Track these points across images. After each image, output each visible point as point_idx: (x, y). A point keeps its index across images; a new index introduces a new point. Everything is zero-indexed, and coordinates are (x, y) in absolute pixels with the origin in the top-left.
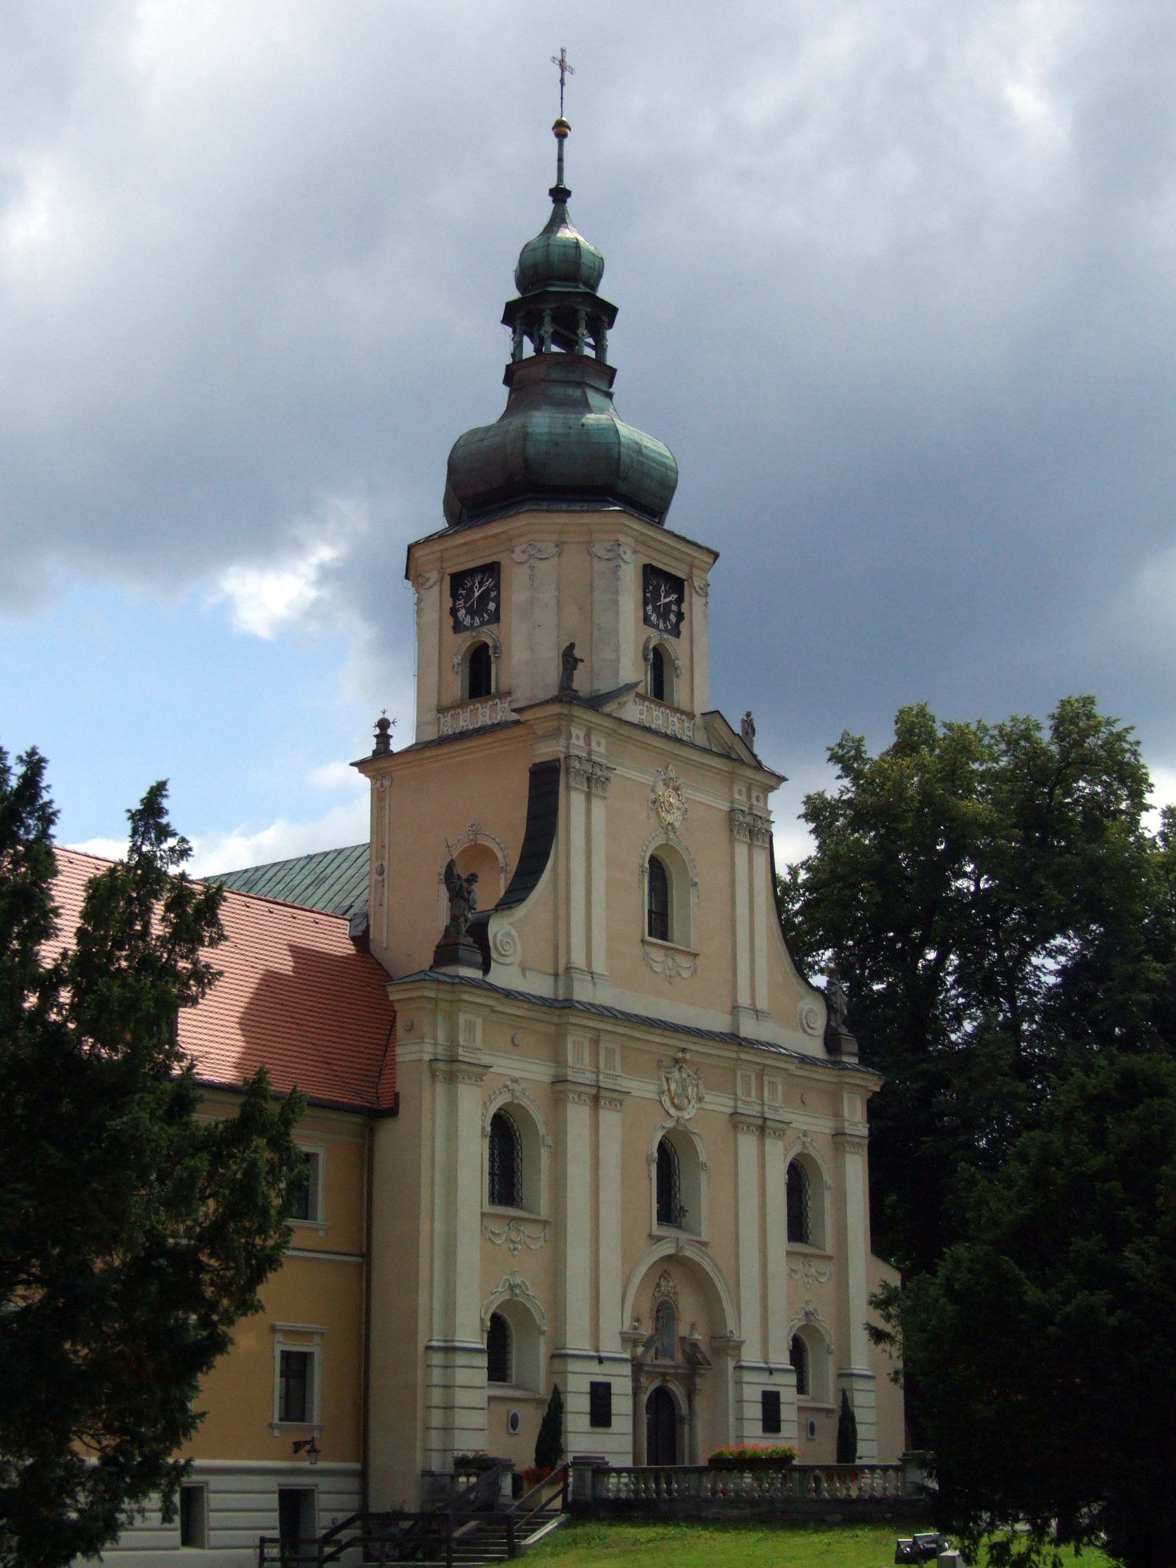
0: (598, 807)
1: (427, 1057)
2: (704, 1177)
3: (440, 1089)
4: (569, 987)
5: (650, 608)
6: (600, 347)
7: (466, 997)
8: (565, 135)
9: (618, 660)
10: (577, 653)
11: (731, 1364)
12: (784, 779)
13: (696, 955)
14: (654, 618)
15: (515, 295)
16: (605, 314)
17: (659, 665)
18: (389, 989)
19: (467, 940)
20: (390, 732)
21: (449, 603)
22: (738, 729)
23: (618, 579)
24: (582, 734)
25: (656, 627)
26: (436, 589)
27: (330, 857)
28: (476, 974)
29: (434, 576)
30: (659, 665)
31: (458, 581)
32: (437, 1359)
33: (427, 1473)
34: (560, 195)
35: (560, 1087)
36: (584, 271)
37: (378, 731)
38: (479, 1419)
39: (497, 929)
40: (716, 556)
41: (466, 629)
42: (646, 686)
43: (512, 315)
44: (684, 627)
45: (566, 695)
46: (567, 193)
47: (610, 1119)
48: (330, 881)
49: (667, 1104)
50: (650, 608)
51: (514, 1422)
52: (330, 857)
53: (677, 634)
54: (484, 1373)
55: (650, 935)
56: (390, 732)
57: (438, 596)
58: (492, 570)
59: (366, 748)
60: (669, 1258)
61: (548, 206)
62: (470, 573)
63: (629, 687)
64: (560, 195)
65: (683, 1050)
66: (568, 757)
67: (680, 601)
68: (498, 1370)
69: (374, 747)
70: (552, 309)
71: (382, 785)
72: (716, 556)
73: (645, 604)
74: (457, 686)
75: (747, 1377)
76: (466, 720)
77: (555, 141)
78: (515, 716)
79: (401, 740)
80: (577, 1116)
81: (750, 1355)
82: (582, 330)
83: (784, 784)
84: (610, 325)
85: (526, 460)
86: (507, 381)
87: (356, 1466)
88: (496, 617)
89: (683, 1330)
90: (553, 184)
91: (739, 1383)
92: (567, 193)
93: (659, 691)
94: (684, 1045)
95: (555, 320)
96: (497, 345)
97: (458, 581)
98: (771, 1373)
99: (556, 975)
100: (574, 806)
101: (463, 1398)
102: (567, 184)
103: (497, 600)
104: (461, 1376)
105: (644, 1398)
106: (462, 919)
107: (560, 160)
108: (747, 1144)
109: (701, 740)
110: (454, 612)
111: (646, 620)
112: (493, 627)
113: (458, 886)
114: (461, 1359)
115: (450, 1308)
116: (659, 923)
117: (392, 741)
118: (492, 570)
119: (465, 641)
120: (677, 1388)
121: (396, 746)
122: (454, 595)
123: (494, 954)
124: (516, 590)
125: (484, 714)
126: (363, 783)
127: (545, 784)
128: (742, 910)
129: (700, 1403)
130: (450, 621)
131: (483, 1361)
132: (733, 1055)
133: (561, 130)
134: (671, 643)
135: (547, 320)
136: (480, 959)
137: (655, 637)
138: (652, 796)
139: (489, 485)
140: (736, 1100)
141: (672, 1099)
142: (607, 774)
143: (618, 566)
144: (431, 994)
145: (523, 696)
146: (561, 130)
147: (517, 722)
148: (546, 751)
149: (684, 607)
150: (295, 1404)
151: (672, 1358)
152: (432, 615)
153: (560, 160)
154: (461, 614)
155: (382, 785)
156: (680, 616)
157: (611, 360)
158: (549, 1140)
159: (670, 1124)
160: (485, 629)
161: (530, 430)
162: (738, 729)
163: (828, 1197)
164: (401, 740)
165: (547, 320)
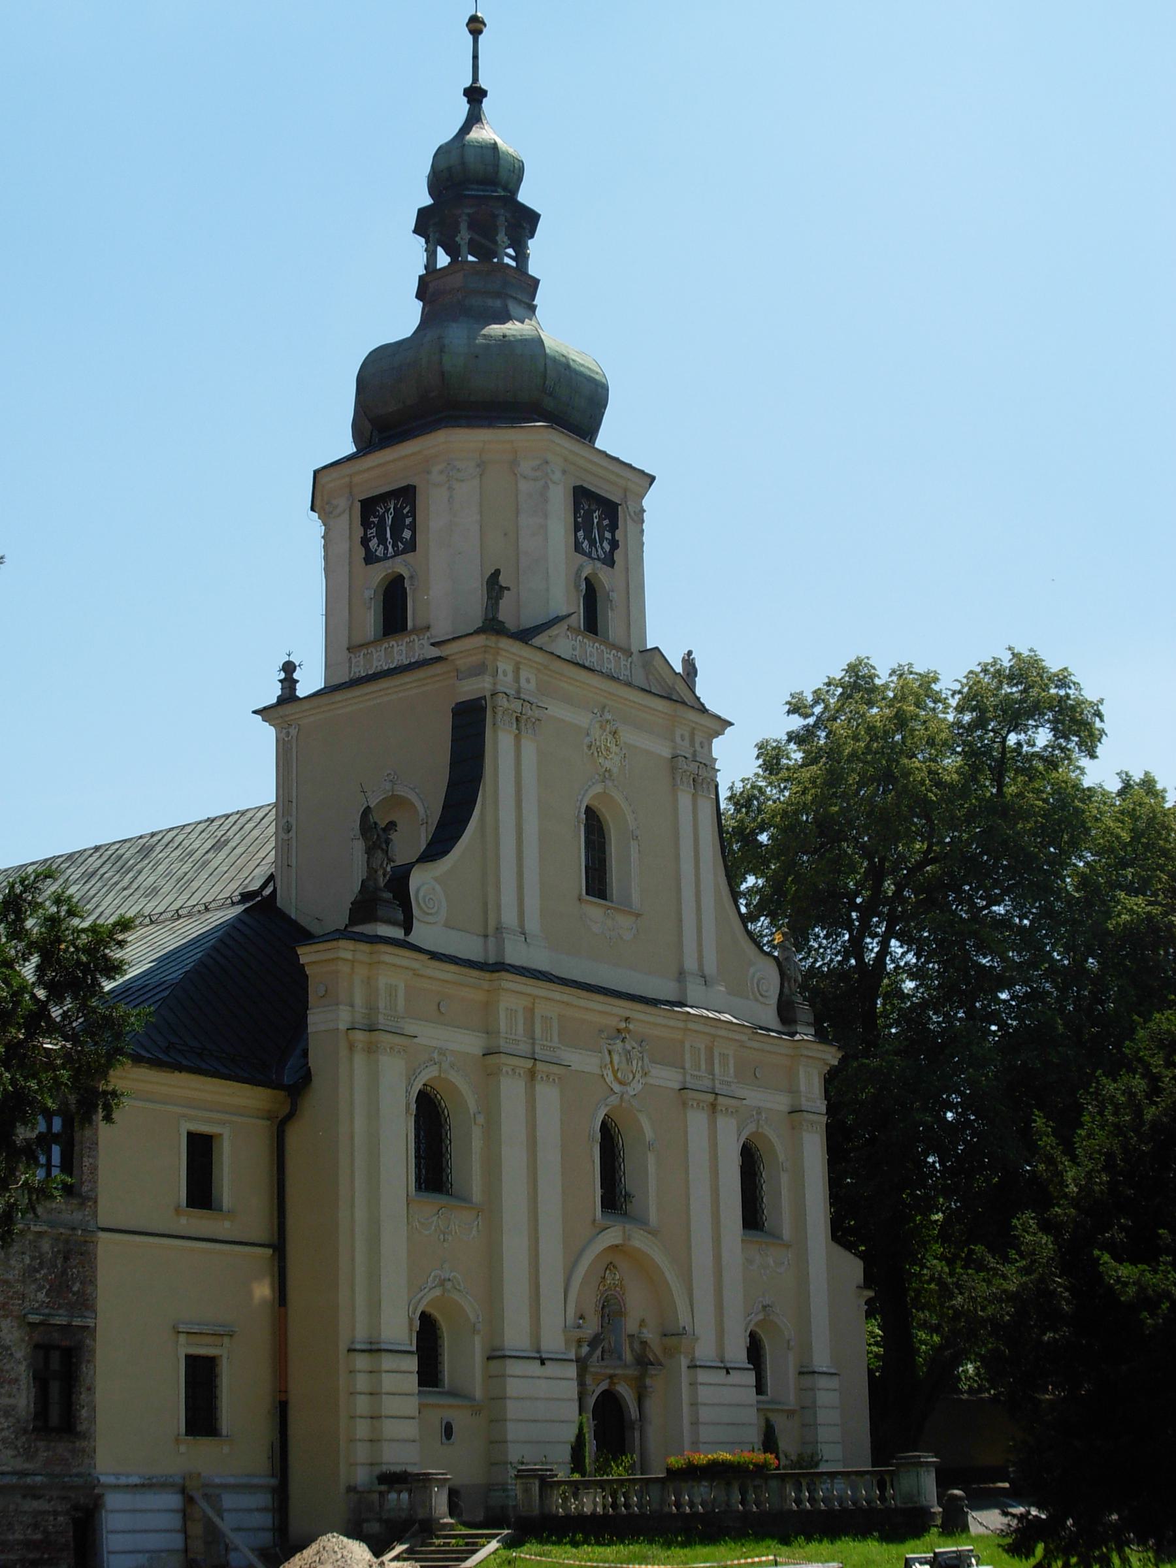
0: (529, 748)
1: (342, 1026)
2: (651, 1159)
3: (359, 1059)
4: (500, 948)
5: (581, 534)
6: (522, 257)
7: (387, 958)
8: (480, 32)
9: (547, 590)
10: (503, 580)
11: (684, 1362)
12: (731, 724)
13: (638, 915)
14: (586, 545)
15: (428, 201)
16: (527, 221)
17: (591, 597)
18: (300, 951)
19: (384, 901)
20: (295, 676)
21: (359, 532)
22: (679, 668)
23: (546, 501)
24: (510, 669)
25: (589, 556)
26: (346, 516)
27: (232, 819)
28: (398, 933)
29: (342, 503)
30: (591, 597)
31: (369, 507)
32: (362, 1362)
33: (351, 1489)
34: (475, 95)
35: (492, 1059)
36: (503, 175)
37: (282, 675)
38: (410, 1429)
39: (421, 881)
40: (652, 479)
41: (378, 560)
42: (579, 619)
43: (425, 223)
44: (618, 555)
45: (492, 626)
46: (484, 93)
48: (232, 844)
49: (610, 1078)
50: (581, 534)
51: (448, 1431)
52: (232, 819)
53: (610, 562)
54: (415, 1378)
55: (587, 894)
56: (295, 676)
57: (349, 522)
58: (407, 494)
59: (272, 693)
60: (614, 1248)
61: (464, 106)
62: (383, 498)
63: (558, 620)
64: (475, 95)
65: (627, 1019)
66: (494, 694)
67: (614, 527)
68: (429, 1374)
69: (279, 693)
70: (468, 215)
71: (288, 734)
72: (652, 479)
73: (576, 530)
74: (370, 621)
75: (703, 1376)
76: (379, 659)
77: (471, 37)
78: (435, 652)
79: (310, 681)
80: (512, 1090)
81: (705, 1350)
82: (502, 238)
83: (729, 730)
84: (532, 237)
85: (443, 374)
86: (420, 295)
87: (274, 1482)
88: (411, 546)
89: (631, 1326)
90: (468, 83)
91: (693, 1384)
92: (484, 93)
93: (592, 625)
94: (628, 1014)
95: (471, 227)
96: (412, 256)
97: (369, 507)
98: (728, 1373)
99: (486, 936)
100: (502, 747)
101: (390, 1405)
102: (483, 83)
103: (413, 528)
104: (388, 1382)
105: (591, 1401)
106: (380, 872)
107: (475, 57)
109: (639, 679)
110: (365, 542)
111: (578, 547)
112: (409, 557)
113: (375, 834)
114: (388, 1362)
115: (375, 1307)
116: (597, 882)
117: (298, 685)
118: (407, 494)
119: (378, 574)
120: (626, 1391)
121: (302, 691)
122: (366, 524)
123: (416, 911)
124: (435, 516)
125: (399, 651)
126: (267, 734)
127: (469, 724)
128: (687, 867)
129: (653, 1407)
130: (361, 553)
131: (412, 1364)
133: (476, 26)
135: (463, 227)
136: (401, 917)
138: (587, 740)
139: (400, 401)
140: (684, 1074)
141: (615, 1072)
142: (537, 713)
143: (546, 487)
144: (349, 956)
145: (442, 628)
146: (476, 26)
147: (439, 659)
148: (469, 689)
149: (619, 535)
150: (202, 1416)
152: (343, 547)
153: (475, 57)
154: (373, 544)
155: (288, 734)
156: (614, 544)
157: (533, 270)
158: (481, 1119)
159: (613, 1100)
160: (399, 559)
161: (446, 341)
162: (679, 668)
163: (785, 1179)
164: (310, 681)
165: (463, 227)
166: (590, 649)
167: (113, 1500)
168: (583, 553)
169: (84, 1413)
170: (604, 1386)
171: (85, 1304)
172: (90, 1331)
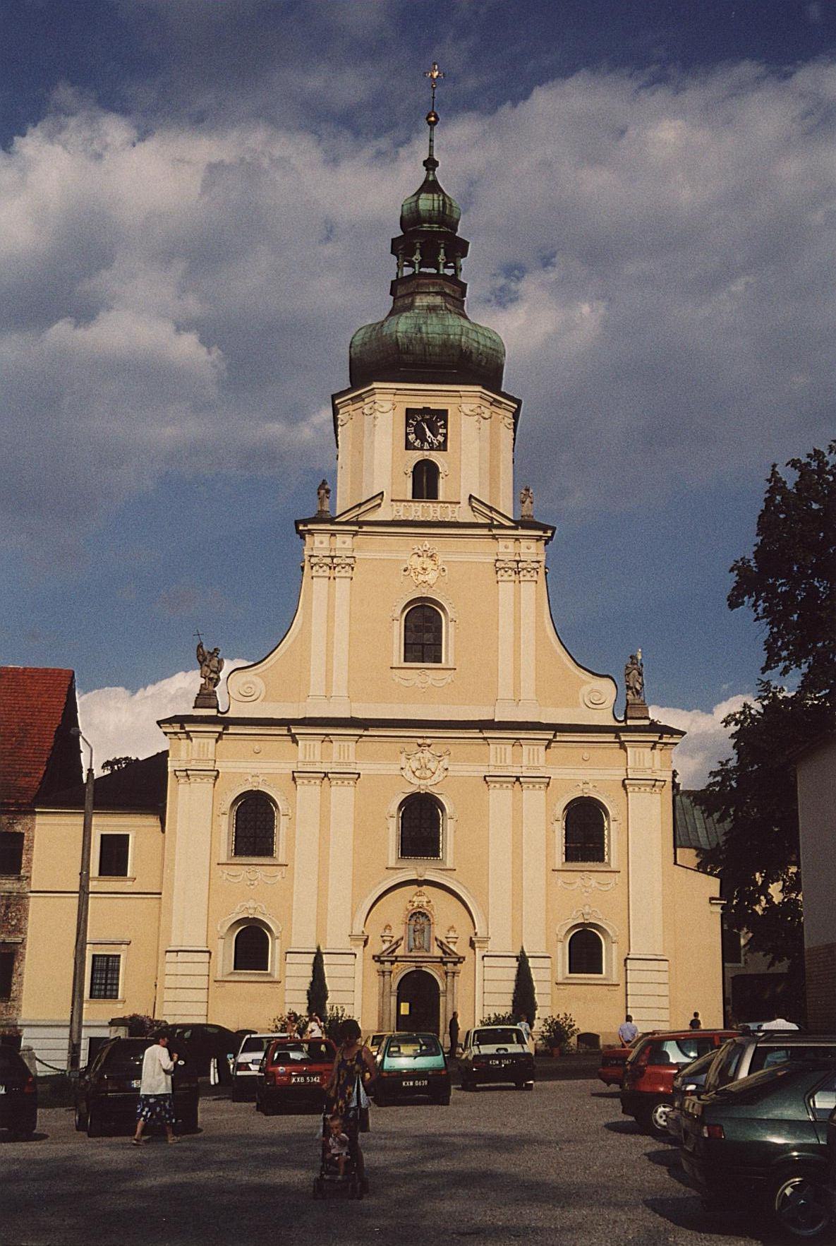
0: (342, 586)
25: (422, 449)
47: (342, 795)
49: (409, 775)
50: (412, 437)
89: (439, 932)
92: (436, 164)
108: (500, 798)
109: (468, 517)
111: (409, 446)
120: (434, 971)
132: (481, 735)
134: (435, 456)
137: (417, 456)
151: (428, 951)
156: (445, 435)
166: (419, 511)
167: (26, 1033)
168: (415, 449)
169: (14, 988)
170: (411, 967)
171: (19, 929)
172: (22, 943)
